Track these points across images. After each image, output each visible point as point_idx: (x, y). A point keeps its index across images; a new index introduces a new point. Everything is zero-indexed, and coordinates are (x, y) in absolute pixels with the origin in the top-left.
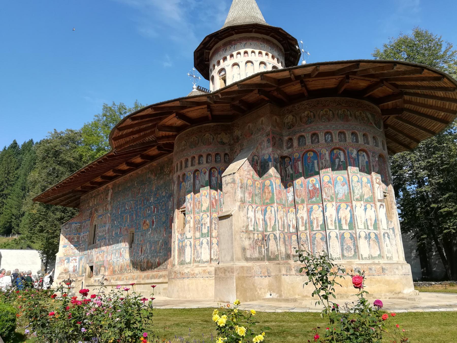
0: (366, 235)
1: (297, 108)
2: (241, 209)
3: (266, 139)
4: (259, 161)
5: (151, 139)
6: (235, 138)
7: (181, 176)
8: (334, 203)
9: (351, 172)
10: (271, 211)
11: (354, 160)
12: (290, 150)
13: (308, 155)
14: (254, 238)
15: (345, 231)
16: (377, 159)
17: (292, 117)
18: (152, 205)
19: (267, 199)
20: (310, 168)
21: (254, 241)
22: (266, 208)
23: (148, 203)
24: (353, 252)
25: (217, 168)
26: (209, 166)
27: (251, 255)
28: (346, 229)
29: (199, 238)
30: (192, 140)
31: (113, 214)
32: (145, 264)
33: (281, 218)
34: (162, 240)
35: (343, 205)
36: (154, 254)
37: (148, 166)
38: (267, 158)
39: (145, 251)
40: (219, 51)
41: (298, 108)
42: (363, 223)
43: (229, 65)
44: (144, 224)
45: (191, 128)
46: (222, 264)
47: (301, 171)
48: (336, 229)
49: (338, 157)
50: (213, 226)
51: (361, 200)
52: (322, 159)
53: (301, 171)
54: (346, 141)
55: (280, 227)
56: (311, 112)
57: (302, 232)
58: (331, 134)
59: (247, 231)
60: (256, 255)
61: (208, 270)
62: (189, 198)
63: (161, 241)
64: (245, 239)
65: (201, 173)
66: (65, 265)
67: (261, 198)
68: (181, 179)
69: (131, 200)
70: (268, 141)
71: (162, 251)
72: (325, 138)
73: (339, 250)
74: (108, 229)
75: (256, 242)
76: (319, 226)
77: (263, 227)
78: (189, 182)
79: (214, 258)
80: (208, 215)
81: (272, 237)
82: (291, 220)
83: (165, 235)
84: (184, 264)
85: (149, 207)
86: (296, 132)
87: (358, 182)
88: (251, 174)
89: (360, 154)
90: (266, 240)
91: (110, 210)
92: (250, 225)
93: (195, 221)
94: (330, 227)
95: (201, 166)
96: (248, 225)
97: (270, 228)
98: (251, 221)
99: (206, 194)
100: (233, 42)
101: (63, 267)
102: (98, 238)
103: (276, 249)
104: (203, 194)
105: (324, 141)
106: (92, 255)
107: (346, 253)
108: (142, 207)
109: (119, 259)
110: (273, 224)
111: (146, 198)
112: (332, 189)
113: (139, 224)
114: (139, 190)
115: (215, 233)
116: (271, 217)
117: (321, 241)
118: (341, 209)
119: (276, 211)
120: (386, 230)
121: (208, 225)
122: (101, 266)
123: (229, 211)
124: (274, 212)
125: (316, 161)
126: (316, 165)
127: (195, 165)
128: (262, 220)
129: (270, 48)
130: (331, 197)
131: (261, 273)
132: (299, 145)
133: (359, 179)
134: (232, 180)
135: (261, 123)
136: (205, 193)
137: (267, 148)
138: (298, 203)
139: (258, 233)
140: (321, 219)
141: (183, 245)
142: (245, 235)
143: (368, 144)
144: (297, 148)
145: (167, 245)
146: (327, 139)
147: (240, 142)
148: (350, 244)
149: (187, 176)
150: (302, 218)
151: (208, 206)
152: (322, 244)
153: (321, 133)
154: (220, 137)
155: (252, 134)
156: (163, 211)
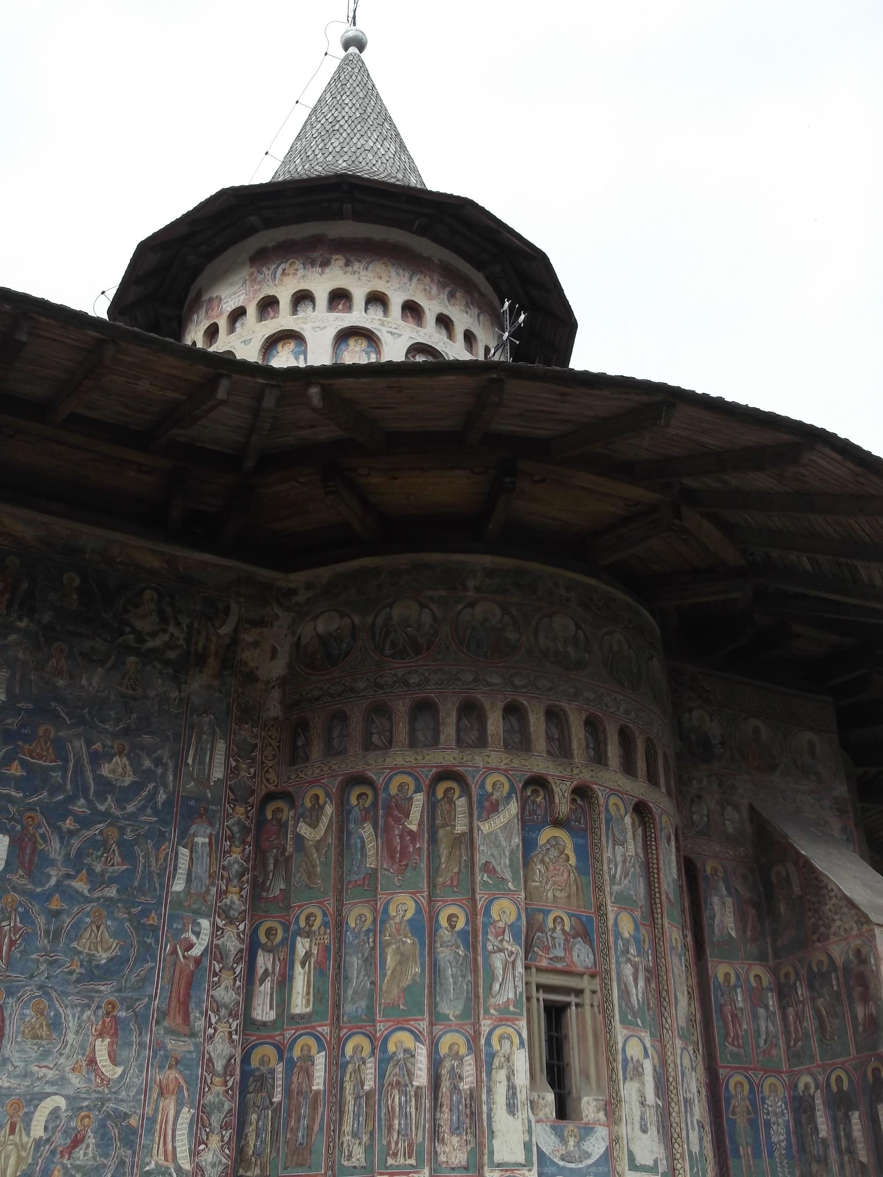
149: (607, 811)
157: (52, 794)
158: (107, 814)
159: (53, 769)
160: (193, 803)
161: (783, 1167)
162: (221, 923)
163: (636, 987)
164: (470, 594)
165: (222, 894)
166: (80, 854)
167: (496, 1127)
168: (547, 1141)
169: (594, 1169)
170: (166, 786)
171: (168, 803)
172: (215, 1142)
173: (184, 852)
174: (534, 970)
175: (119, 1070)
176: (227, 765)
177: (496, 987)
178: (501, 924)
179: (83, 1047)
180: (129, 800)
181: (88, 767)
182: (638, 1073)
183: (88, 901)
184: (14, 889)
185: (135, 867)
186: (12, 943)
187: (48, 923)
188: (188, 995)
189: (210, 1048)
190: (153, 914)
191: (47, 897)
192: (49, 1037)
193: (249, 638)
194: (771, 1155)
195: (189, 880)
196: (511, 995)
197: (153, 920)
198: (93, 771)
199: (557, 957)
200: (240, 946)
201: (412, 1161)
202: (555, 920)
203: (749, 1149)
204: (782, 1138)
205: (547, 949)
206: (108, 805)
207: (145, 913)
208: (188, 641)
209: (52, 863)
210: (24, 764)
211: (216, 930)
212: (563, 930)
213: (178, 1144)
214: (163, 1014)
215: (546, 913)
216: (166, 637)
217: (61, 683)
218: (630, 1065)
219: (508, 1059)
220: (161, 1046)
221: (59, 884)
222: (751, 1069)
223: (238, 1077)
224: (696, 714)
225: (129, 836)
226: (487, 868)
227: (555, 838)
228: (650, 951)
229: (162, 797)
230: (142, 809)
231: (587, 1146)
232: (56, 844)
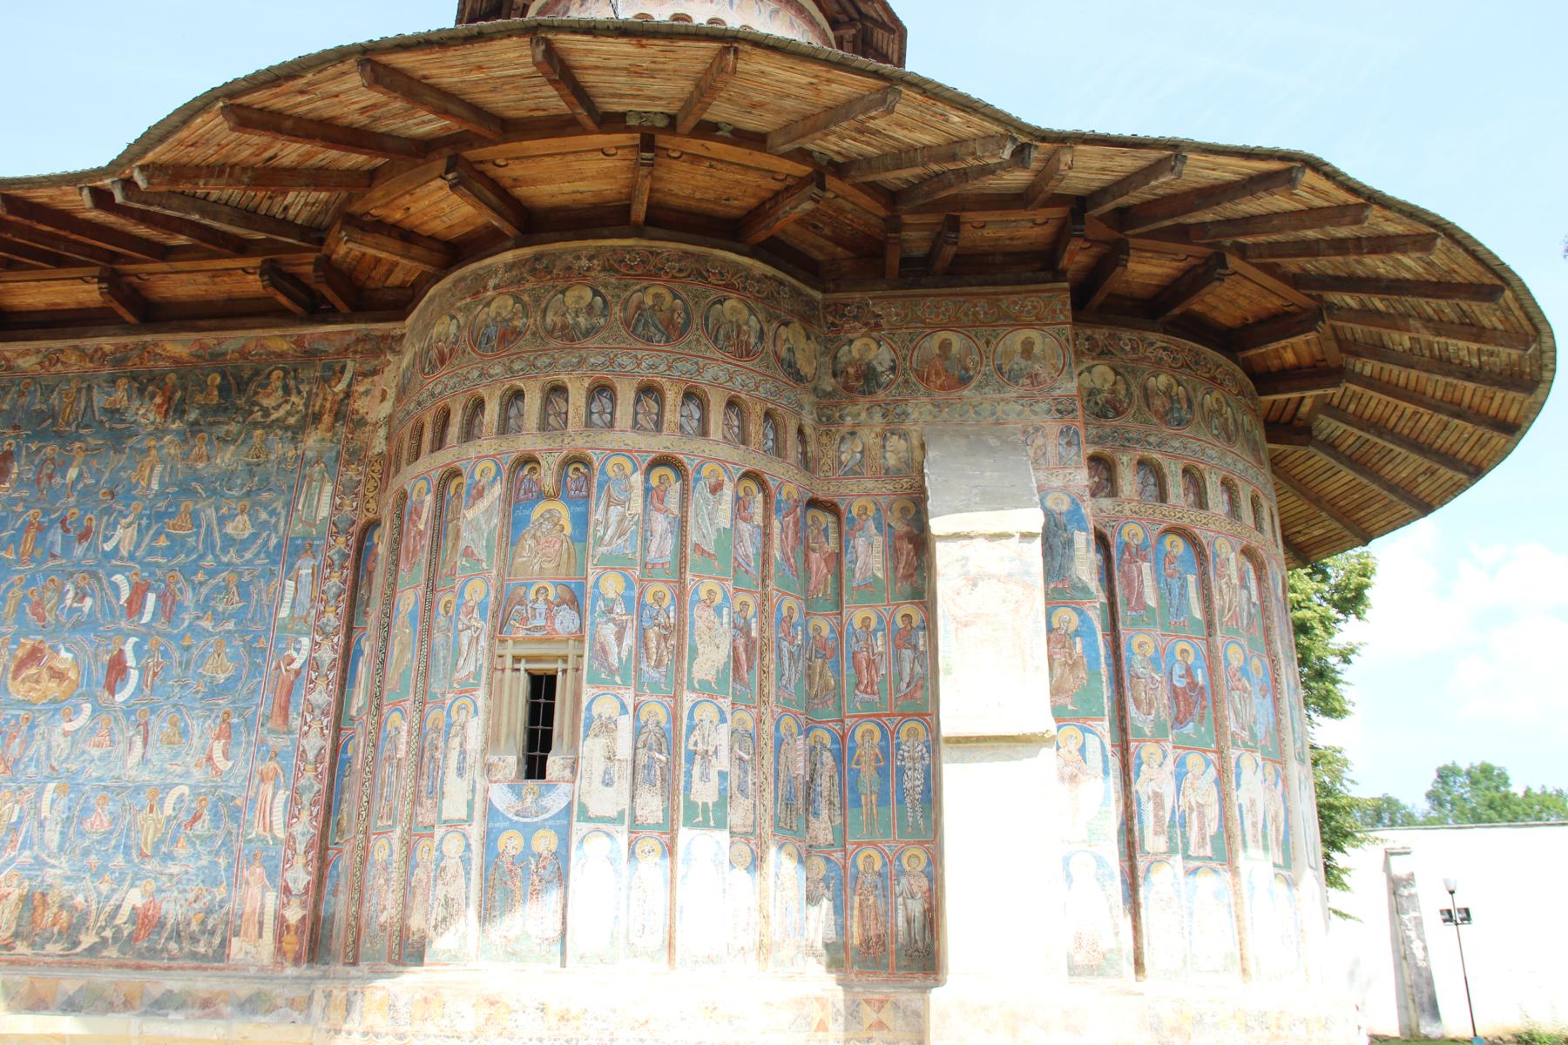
1: (1128, 348)
3: (1053, 427)
10: (1082, 750)
17: (1111, 376)
20: (1175, 602)
30: (649, 301)
34: (193, 787)
41: (1132, 349)
44: (22, 665)
45: (645, 243)
52: (1221, 577)
53: (1151, 599)
56: (1179, 384)
62: (611, 595)
65: (697, 480)
71: (182, 851)
78: (615, 511)
80: (721, 712)
85: (94, 575)
86: (1129, 440)
93: (637, 732)
99: (718, 599)
104: (703, 595)
108: (19, 561)
115: (741, 813)
124: (1099, 757)
135: (1018, 347)
136: (710, 592)
137: (1062, 463)
138: (1139, 731)
140: (1213, 812)
145: (235, 819)
147: (881, 395)
149: (603, 472)
150: (1158, 798)
151: (726, 664)
154: (787, 340)
155: (964, 381)
157: (187, 556)
158: (229, 564)
159: (189, 536)
160: (299, 542)
161: (914, 811)
162: (318, 638)
163: (620, 643)
164: (489, 293)
165: (320, 615)
166: (207, 599)
167: (447, 788)
168: (502, 797)
169: (550, 822)
170: (277, 532)
171: (279, 546)
172: (305, 816)
173: (290, 584)
174: (510, 642)
175: (230, 764)
176: (333, 505)
177: (461, 662)
178: (471, 604)
179: (203, 748)
180: (247, 549)
181: (216, 528)
182: (609, 727)
183: (212, 635)
184: (158, 633)
185: (249, 602)
186: (155, 674)
187: (182, 656)
188: (288, 701)
189: (304, 742)
190: (263, 639)
192: (179, 742)
193: (361, 389)
194: (901, 801)
195: (293, 607)
196: (472, 669)
197: (262, 643)
198: (220, 531)
199: (536, 627)
200: (334, 656)
201: (390, 823)
202: (537, 592)
203: (874, 797)
204: (917, 783)
205: (525, 620)
206: (231, 556)
207: (256, 638)
208: (307, 406)
209: (186, 609)
210: (168, 536)
211: (316, 645)
212: (546, 600)
213: (274, 818)
214: (268, 718)
215: (528, 586)
216: (288, 407)
217: (200, 465)
218: (597, 723)
219: (463, 728)
220: (263, 742)
221: (190, 623)
222: (886, 715)
223: (327, 764)
224: (857, 344)
225: (246, 578)
226: (468, 553)
227: (549, 511)
228: (672, 608)
229: (274, 541)
230: (257, 555)
231: (545, 802)
232: (190, 594)
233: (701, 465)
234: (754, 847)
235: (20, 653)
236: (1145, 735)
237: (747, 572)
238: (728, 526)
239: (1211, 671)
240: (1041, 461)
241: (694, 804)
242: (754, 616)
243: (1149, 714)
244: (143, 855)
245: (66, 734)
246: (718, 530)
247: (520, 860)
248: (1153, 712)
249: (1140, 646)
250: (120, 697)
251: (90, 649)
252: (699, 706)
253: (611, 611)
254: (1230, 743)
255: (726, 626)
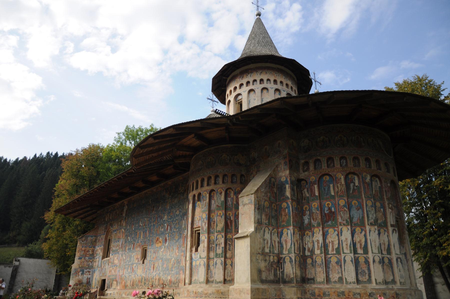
0: (380, 259)
2: (258, 231)
3: (283, 162)
4: (276, 183)
5: (168, 159)
6: (252, 160)
7: (196, 196)
8: (349, 227)
9: (365, 197)
10: (287, 234)
11: (368, 185)
12: (306, 173)
13: (324, 179)
14: (270, 261)
15: (359, 255)
16: (389, 185)
18: (166, 223)
19: (283, 221)
21: (270, 264)
22: (282, 230)
23: (161, 221)
24: (367, 277)
25: (233, 189)
26: (225, 186)
27: (266, 277)
28: (360, 253)
29: (213, 258)
30: (209, 160)
31: (127, 230)
32: (157, 281)
33: (297, 241)
34: (174, 258)
35: (358, 229)
36: (166, 271)
37: (163, 185)
38: (284, 180)
39: (157, 268)
40: (236, 78)
42: (377, 247)
43: (246, 91)
44: (157, 241)
46: (237, 285)
47: (317, 194)
48: (351, 253)
49: (352, 181)
50: (228, 246)
51: (375, 225)
52: (338, 183)
54: (360, 166)
55: (296, 250)
57: (318, 255)
58: (345, 158)
59: (263, 254)
60: (272, 277)
61: (222, 291)
62: (204, 218)
63: (173, 259)
64: (261, 262)
65: (217, 193)
66: (80, 277)
67: (277, 220)
68: (196, 198)
69: (145, 217)
70: (285, 163)
71: (174, 269)
72: (340, 163)
73: (353, 274)
74: (122, 244)
75: (271, 264)
76: (335, 249)
77: (278, 249)
78: (204, 202)
79: (228, 279)
80: (222, 236)
81: (287, 260)
82: (307, 243)
83: (177, 254)
84: (197, 283)
85: (163, 225)
87: (372, 206)
88: (268, 196)
89: (373, 179)
90: (281, 263)
91: (124, 225)
92: (266, 247)
94: (345, 251)
95: (218, 186)
96: (264, 247)
97: (286, 250)
98: (267, 243)
99: (222, 214)
100: (250, 71)
101: (77, 278)
102: (111, 252)
103: (292, 272)
104: (219, 214)
105: (339, 166)
106: (105, 269)
107: (360, 278)
108: (156, 224)
109: (130, 274)
110: (289, 246)
111: (159, 216)
112: (347, 213)
113: (152, 241)
114: (154, 207)
116: (287, 240)
117: (336, 265)
118: (356, 233)
119: (292, 234)
120: (399, 255)
121: (223, 245)
122: (113, 280)
123: (246, 232)
124: (290, 235)
125: (331, 185)
126: (332, 189)
127: (211, 185)
128: (278, 243)
129: (284, 77)
130: (347, 220)
131: (275, 296)
132: (315, 168)
133: (373, 204)
134: (249, 201)
136: (220, 213)
137: (284, 170)
138: (314, 226)
139: (274, 255)
140: (336, 243)
141: (197, 264)
142: (261, 257)
143: (380, 169)
144: (313, 172)
145: (179, 263)
146: (342, 163)
148: (365, 268)
149: (203, 195)
150: (318, 241)
151: (223, 227)
152: (337, 268)
153: (337, 158)
156: (176, 229)
158: (177, 219)
163: (205, 226)
173: (184, 221)
182: (204, 242)
191: (172, 233)
197: (181, 233)
205: (196, 224)
207: (180, 232)
210: (170, 216)
214: (182, 245)
217: (173, 203)
218: (202, 241)
224: (252, 154)
229: (181, 214)
232: (173, 225)
233: (218, 190)
234: (232, 260)
235: (156, 239)
236: (315, 226)
237: (230, 207)
238: (223, 200)
239: (335, 208)
240: (281, 170)
241: (217, 254)
242: (232, 216)
243: (316, 221)
244: (170, 271)
245: (161, 252)
246: (221, 201)
247: (195, 266)
248: (317, 221)
249: (314, 205)
250: (167, 245)
251: (163, 237)
252: (218, 235)
253: (204, 220)
254: (339, 225)
255: (223, 219)
